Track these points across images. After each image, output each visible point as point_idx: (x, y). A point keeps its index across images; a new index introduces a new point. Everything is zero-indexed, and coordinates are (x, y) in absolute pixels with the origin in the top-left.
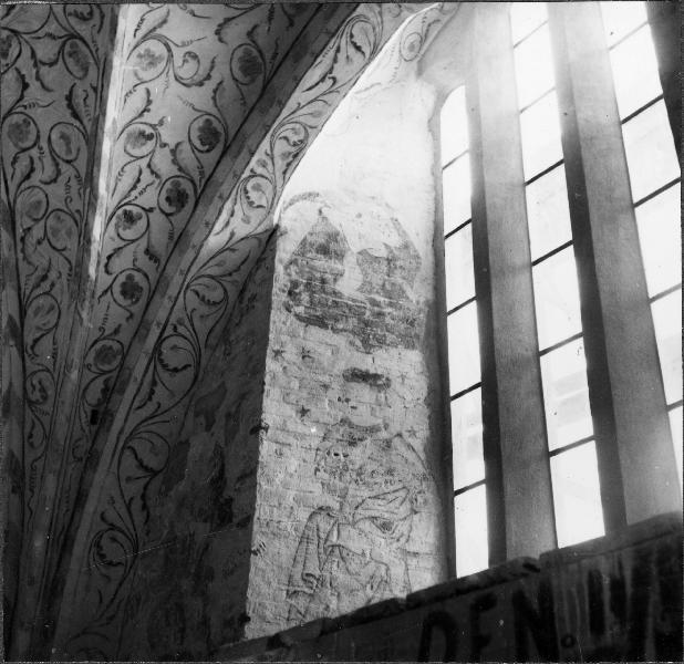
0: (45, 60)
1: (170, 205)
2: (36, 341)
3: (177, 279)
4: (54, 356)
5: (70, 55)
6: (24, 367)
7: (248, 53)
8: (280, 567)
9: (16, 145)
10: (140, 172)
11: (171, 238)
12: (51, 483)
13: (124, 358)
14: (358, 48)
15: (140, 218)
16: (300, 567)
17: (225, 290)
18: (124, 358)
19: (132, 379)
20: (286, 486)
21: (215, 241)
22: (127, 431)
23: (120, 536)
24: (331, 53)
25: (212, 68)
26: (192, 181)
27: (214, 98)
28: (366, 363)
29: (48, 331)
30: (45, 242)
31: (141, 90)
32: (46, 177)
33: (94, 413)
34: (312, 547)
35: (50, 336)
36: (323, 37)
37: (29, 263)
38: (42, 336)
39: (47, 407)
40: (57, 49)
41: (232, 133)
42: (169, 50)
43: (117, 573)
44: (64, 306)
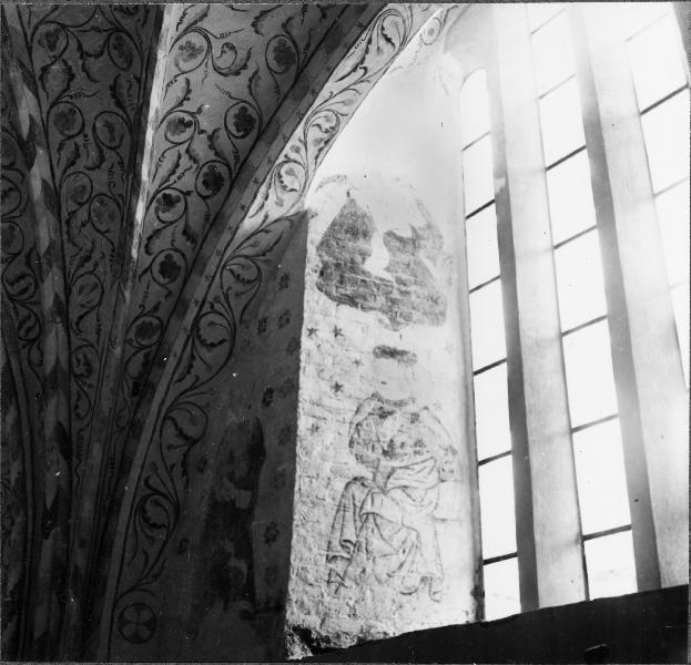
0: (91, 52)
1: (207, 187)
2: (81, 317)
3: (214, 260)
4: (98, 332)
5: (115, 48)
7: (281, 43)
8: (320, 534)
9: (62, 133)
10: (179, 157)
11: (207, 219)
12: (97, 450)
13: (162, 334)
14: (389, 40)
15: (178, 200)
16: (338, 534)
17: (259, 269)
18: (162, 334)
20: (324, 458)
21: (250, 223)
22: (168, 403)
23: (163, 500)
24: (363, 45)
25: (248, 58)
26: (228, 166)
27: (249, 87)
28: (392, 341)
30: (89, 225)
31: (181, 79)
32: (90, 164)
33: (136, 385)
34: (349, 515)
35: (94, 313)
36: (356, 30)
37: (74, 244)
38: (86, 313)
39: (93, 380)
40: (101, 43)
41: (266, 119)
42: (209, 42)
43: (161, 535)
44: (107, 285)
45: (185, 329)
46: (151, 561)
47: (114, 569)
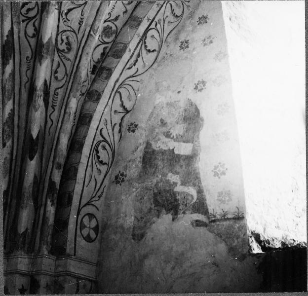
2: (70, 10)
4: (80, 23)
6: (58, 26)
18: (116, 37)
19: (127, 50)
23: (107, 147)
29: (80, 6)
35: (80, 9)
39: (71, 56)
43: (104, 168)
45: (138, 35)
46: (98, 185)
47: (78, 188)
